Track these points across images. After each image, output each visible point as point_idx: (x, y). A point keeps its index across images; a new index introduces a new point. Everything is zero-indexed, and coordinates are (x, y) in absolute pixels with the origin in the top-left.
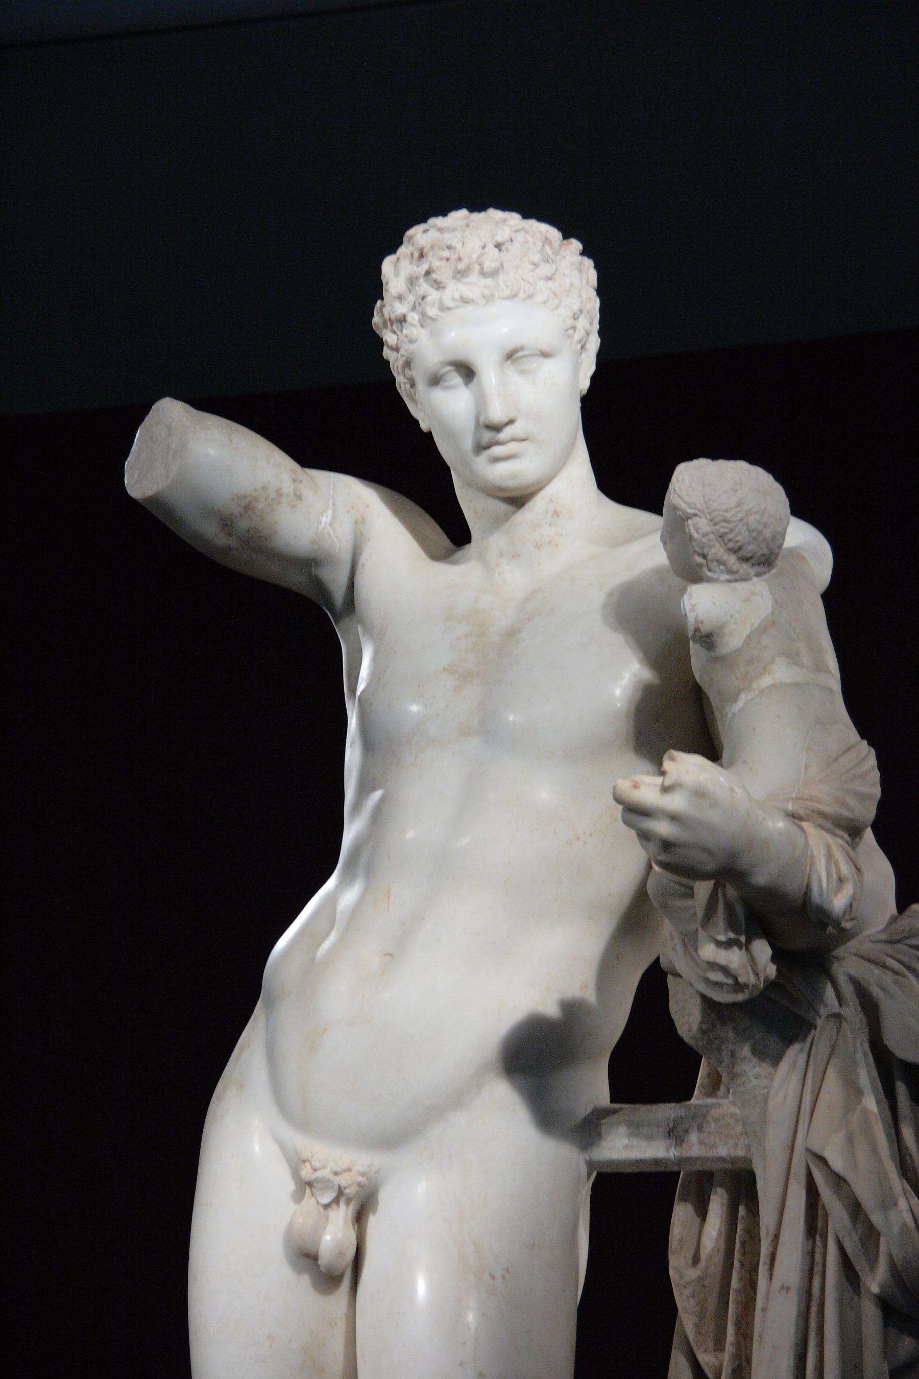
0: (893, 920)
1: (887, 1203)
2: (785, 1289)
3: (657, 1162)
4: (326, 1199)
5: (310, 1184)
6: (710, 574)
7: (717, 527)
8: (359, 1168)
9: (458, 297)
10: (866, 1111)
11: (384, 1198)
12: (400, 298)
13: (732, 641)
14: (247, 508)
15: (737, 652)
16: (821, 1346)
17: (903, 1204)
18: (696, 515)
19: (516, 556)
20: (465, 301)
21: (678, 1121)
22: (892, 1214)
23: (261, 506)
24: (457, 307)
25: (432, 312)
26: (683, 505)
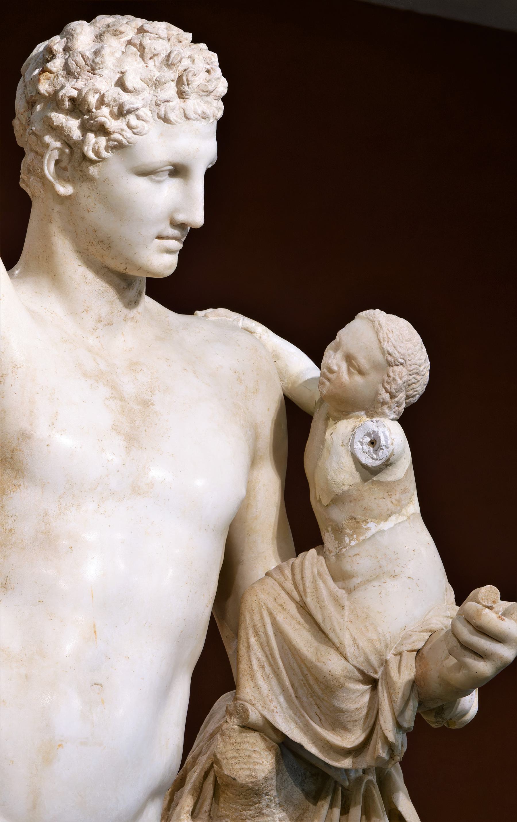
6: (387, 411)
7: (411, 377)
9: (200, 112)
15: (398, 482)
18: (402, 364)
19: (110, 324)
24: (196, 119)
25: (172, 116)
26: (397, 355)
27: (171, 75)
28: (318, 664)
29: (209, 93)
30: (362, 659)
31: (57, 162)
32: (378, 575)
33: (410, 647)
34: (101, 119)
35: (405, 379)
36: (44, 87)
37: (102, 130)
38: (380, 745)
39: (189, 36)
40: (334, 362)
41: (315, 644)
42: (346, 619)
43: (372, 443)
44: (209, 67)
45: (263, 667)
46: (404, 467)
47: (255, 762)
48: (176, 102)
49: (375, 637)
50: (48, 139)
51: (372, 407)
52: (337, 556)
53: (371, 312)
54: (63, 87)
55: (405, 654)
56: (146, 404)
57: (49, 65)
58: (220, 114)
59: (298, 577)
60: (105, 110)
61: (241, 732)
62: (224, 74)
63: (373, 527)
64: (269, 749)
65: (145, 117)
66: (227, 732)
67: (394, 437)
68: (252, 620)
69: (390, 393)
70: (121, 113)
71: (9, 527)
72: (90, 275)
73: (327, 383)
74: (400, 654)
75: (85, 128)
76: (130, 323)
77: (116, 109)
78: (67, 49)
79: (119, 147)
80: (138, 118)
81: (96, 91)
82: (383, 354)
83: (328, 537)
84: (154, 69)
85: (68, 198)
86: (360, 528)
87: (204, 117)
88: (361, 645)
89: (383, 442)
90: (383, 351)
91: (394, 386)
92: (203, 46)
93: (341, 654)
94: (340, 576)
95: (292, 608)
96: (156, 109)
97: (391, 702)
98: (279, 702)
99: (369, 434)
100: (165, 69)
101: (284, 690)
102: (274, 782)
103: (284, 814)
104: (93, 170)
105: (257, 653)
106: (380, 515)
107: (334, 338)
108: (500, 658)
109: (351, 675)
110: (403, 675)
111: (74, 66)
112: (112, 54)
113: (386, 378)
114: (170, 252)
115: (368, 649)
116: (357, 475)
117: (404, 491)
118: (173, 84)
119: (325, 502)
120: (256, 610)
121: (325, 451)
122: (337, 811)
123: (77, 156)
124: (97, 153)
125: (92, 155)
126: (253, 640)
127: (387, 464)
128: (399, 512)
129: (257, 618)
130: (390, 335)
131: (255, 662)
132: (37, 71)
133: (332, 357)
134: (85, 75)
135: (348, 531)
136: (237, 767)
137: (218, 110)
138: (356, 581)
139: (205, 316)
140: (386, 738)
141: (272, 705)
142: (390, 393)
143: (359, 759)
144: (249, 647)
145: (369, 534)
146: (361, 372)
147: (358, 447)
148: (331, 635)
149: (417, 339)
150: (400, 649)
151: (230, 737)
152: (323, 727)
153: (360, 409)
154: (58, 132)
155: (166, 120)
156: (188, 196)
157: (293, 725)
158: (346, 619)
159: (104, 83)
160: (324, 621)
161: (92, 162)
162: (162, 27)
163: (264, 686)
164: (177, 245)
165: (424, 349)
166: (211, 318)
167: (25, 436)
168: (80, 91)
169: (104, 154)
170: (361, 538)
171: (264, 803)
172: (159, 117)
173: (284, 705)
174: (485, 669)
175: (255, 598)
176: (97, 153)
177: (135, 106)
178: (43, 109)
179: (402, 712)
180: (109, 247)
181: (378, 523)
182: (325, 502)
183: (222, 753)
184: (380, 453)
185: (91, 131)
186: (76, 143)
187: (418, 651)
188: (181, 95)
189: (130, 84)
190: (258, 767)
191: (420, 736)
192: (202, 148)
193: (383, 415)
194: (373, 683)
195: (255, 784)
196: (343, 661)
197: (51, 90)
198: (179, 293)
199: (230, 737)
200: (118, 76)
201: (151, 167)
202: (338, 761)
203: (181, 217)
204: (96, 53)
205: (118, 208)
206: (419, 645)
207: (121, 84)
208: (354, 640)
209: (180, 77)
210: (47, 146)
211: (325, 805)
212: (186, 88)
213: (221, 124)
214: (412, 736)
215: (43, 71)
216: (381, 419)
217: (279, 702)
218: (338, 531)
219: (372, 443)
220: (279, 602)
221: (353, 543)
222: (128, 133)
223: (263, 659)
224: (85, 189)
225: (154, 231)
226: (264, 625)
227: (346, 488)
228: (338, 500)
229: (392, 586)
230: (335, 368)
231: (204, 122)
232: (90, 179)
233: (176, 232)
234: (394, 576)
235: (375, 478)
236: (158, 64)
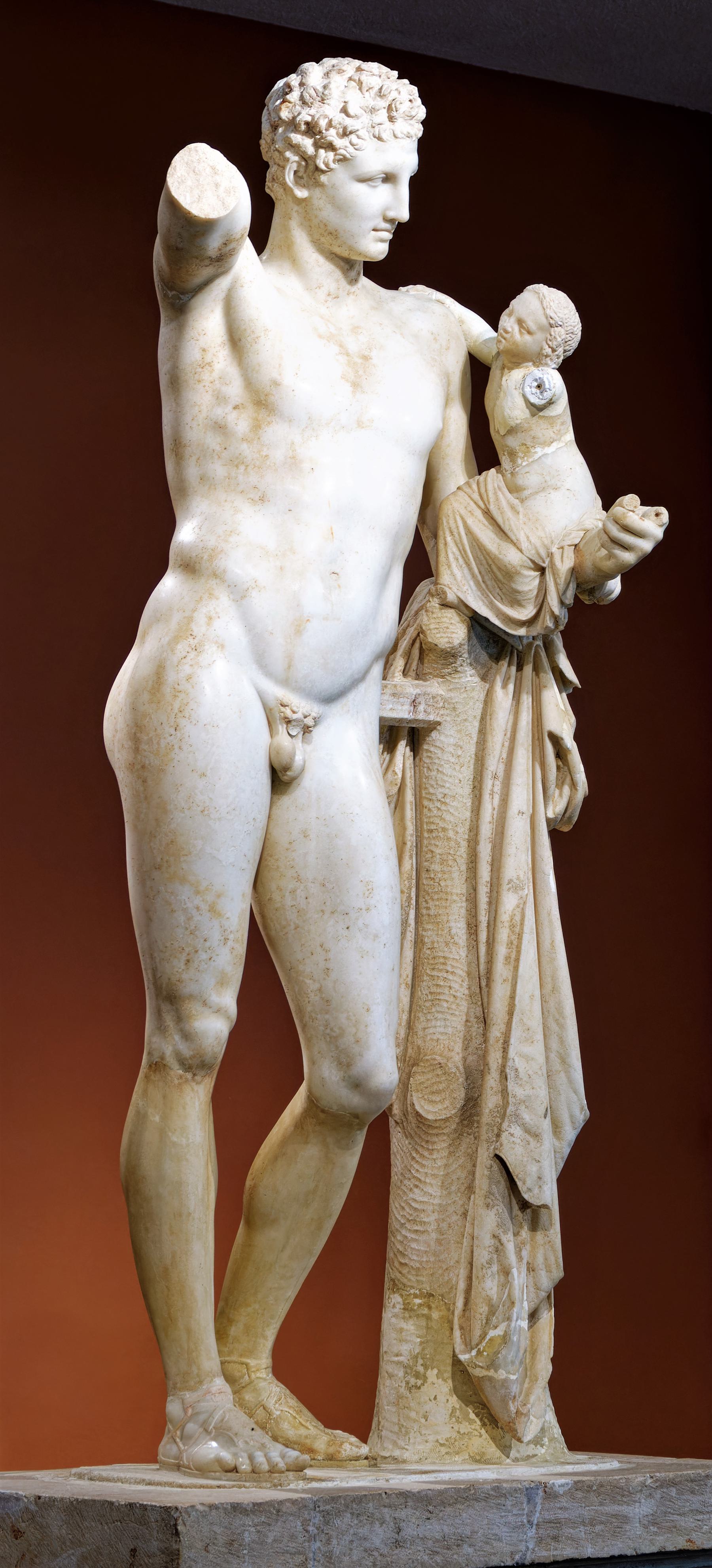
5: (288, 722)
6: (549, 362)
9: (405, 133)
15: (558, 416)
19: (337, 297)
25: (384, 136)
26: (557, 319)
27: (383, 104)
28: (501, 556)
29: (412, 117)
30: (533, 552)
31: (295, 172)
32: (543, 488)
33: (570, 543)
34: (330, 138)
35: (563, 337)
36: (285, 114)
37: (331, 147)
38: (548, 618)
39: (395, 73)
40: (509, 325)
41: (497, 540)
42: (521, 522)
43: (539, 387)
44: (411, 98)
45: (457, 559)
46: (562, 406)
47: (451, 631)
48: (388, 124)
49: (543, 535)
50: (288, 154)
51: (538, 359)
52: (512, 473)
53: (536, 286)
54: (299, 114)
55: (566, 548)
56: (366, 358)
57: (288, 97)
58: (420, 134)
59: (483, 490)
60: (332, 132)
61: (441, 609)
62: (423, 103)
63: (539, 451)
64: (463, 621)
65: (363, 137)
66: (430, 609)
67: (556, 383)
68: (448, 523)
69: (552, 348)
70: (345, 133)
71: (264, 454)
72: (321, 260)
73: (503, 341)
74: (562, 548)
75: (317, 146)
76: (352, 297)
77: (341, 131)
78: (302, 84)
79: (343, 160)
80: (358, 137)
81: (326, 116)
82: (547, 318)
83: (504, 459)
84: (369, 99)
85: (304, 200)
86: (529, 452)
87: (409, 136)
88: (533, 541)
89: (547, 386)
90: (547, 317)
91: (555, 343)
92: (406, 81)
93: (518, 548)
94: (514, 489)
95: (479, 513)
96: (372, 130)
97: (556, 584)
98: (470, 586)
99: (536, 380)
100: (378, 99)
101: (473, 576)
102: (466, 647)
103: (473, 671)
104: (323, 178)
105: (452, 548)
106: (545, 442)
107: (508, 306)
108: (641, 550)
109: (526, 564)
110: (565, 564)
111: (308, 97)
112: (338, 87)
113: (549, 337)
114: (382, 241)
115: (538, 544)
116: (527, 411)
117: (562, 424)
118: (385, 110)
119: (502, 433)
120: (451, 515)
121: (502, 394)
122: (514, 669)
123: (311, 167)
124: (327, 165)
125: (323, 167)
126: (449, 539)
127: (550, 403)
128: (559, 440)
129: (452, 522)
130: (552, 304)
131: (451, 556)
132: (279, 102)
133: (506, 321)
134: (317, 104)
135: (520, 454)
136: (438, 635)
137: (418, 131)
138: (526, 493)
139: (407, 291)
140: (553, 612)
141: (465, 588)
142: (552, 348)
143: (531, 629)
144: (446, 544)
145: (536, 457)
146: (529, 333)
147: (527, 390)
148: (510, 534)
149: (572, 306)
150: (562, 544)
151: (433, 613)
152: (503, 604)
153: (528, 361)
154: (296, 148)
155: (379, 138)
156: (397, 198)
157: (481, 603)
158: (521, 522)
159: (331, 111)
160: (504, 523)
161: (323, 172)
162: (374, 67)
163: (459, 575)
164: (389, 236)
165: (577, 315)
166: (412, 293)
167: (276, 384)
168: (313, 116)
169: (332, 165)
170: (531, 460)
171: (458, 663)
172: (375, 137)
173: (474, 588)
174: (629, 558)
175: (450, 507)
176: (327, 165)
177: (356, 128)
178: (284, 131)
179: (565, 592)
180: (337, 238)
181: (543, 448)
182: (502, 432)
183: (426, 625)
184: (545, 394)
185: (322, 147)
186: (310, 157)
187: (576, 546)
188: (391, 119)
189: (351, 111)
190: (454, 635)
191: (576, 610)
192: (407, 161)
193: (546, 365)
194: (542, 570)
195: (452, 648)
196: (519, 553)
197: (290, 116)
198: (388, 273)
199: (433, 613)
200: (343, 104)
201: (368, 176)
202: (516, 630)
203: (391, 214)
204: (325, 87)
205: (343, 207)
206: (576, 541)
207: (344, 111)
208: (528, 537)
209: (390, 106)
210: (287, 160)
211: (504, 664)
212: (394, 114)
213: (421, 142)
214: (571, 610)
215: (284, 102)
216: (545, 368)
217: (470, 586)
218: (513, 455)
219: (539, 387)
220: (469, 509)
221: (524, 464)
222: (351, 149)
223: (457, 553)
224: (317, 192)
225: (372, 225)
226: (457, 527)
227: (518, 422)
228: (512, 431)
229: (554, 495)
230: (510, 329)
232: (321, 185)
233: (387, 226)
234: (556, 489)
235: (541, 414)
236: (373, 95)
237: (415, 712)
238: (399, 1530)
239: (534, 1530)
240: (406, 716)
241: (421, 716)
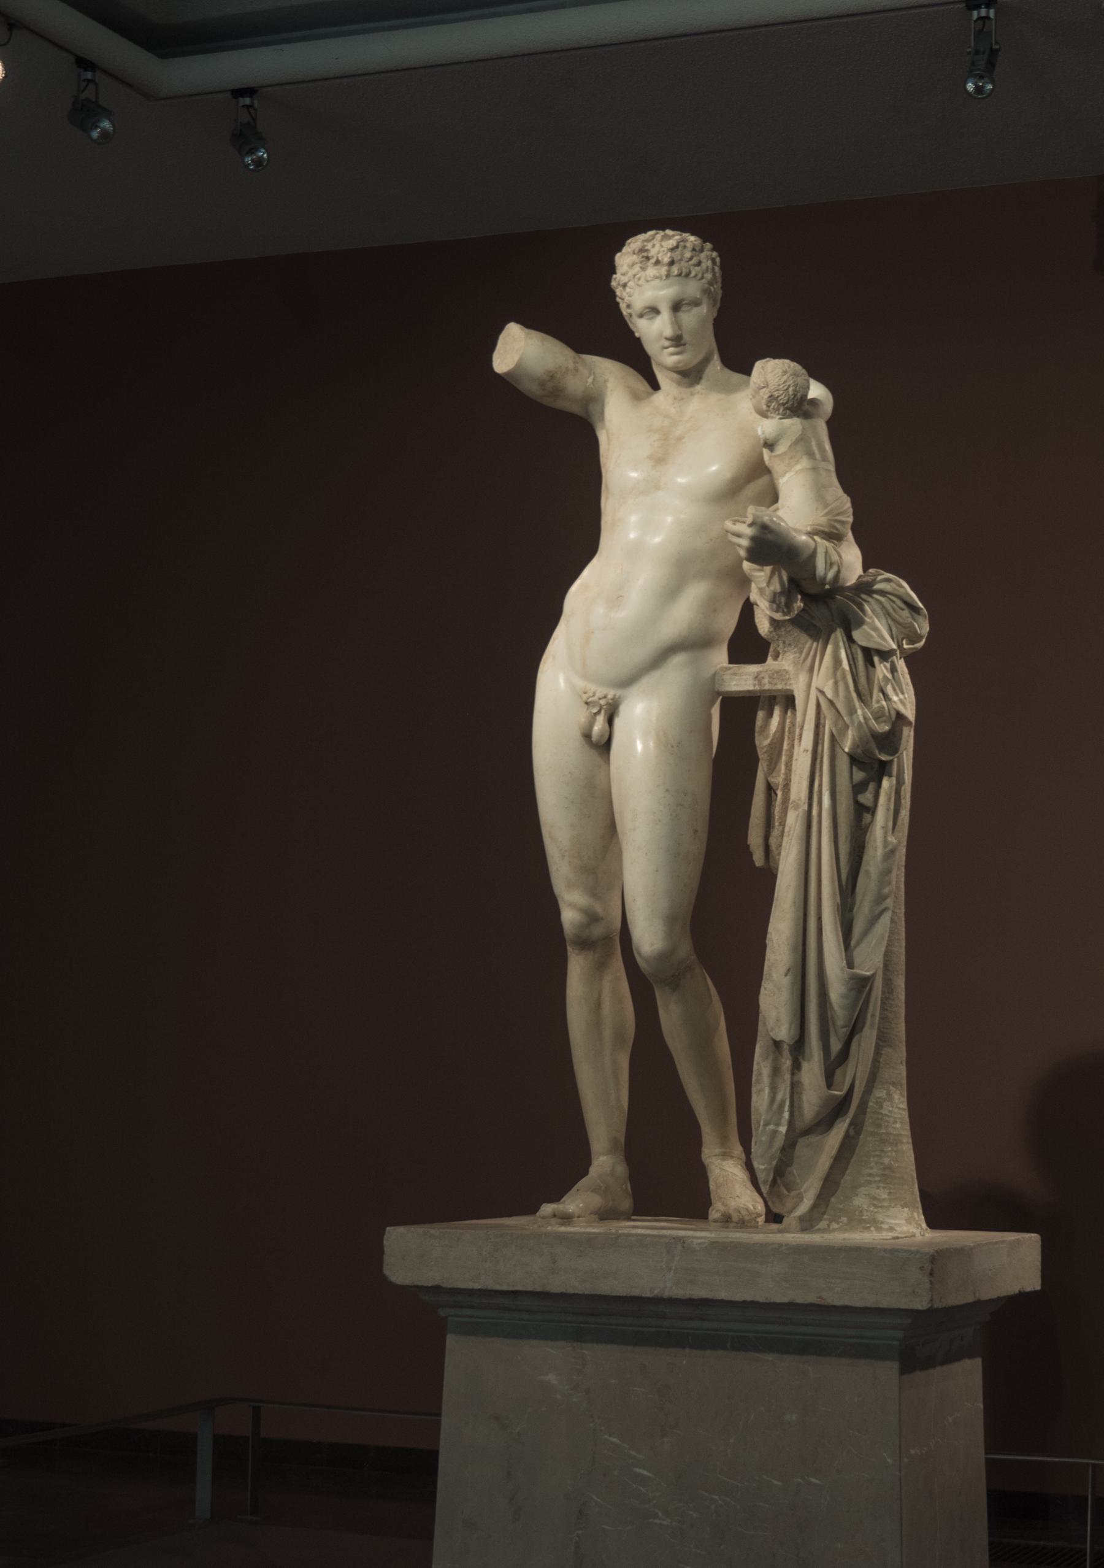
0: (860, 576)
1: (852, 711)
2: (806, 751)
3: (749, 691)
4: (595, 710)
8: (610, 696)
10: (843, 670)
11: (623, 709)
12: (623, 274)
13: (781, 449)
14: (552, 377)
16: (821, 776)
17: (859, 712)
20: (657, 278)
21: (759, 673)
22: (854, 717)
23: (558, 376)
25: (640, 282)
231: (658, 281)
237: (760, 684)
238: (555, 1262)
239: (672, 1273)
240: (751, 688)
241: (767, 687)
